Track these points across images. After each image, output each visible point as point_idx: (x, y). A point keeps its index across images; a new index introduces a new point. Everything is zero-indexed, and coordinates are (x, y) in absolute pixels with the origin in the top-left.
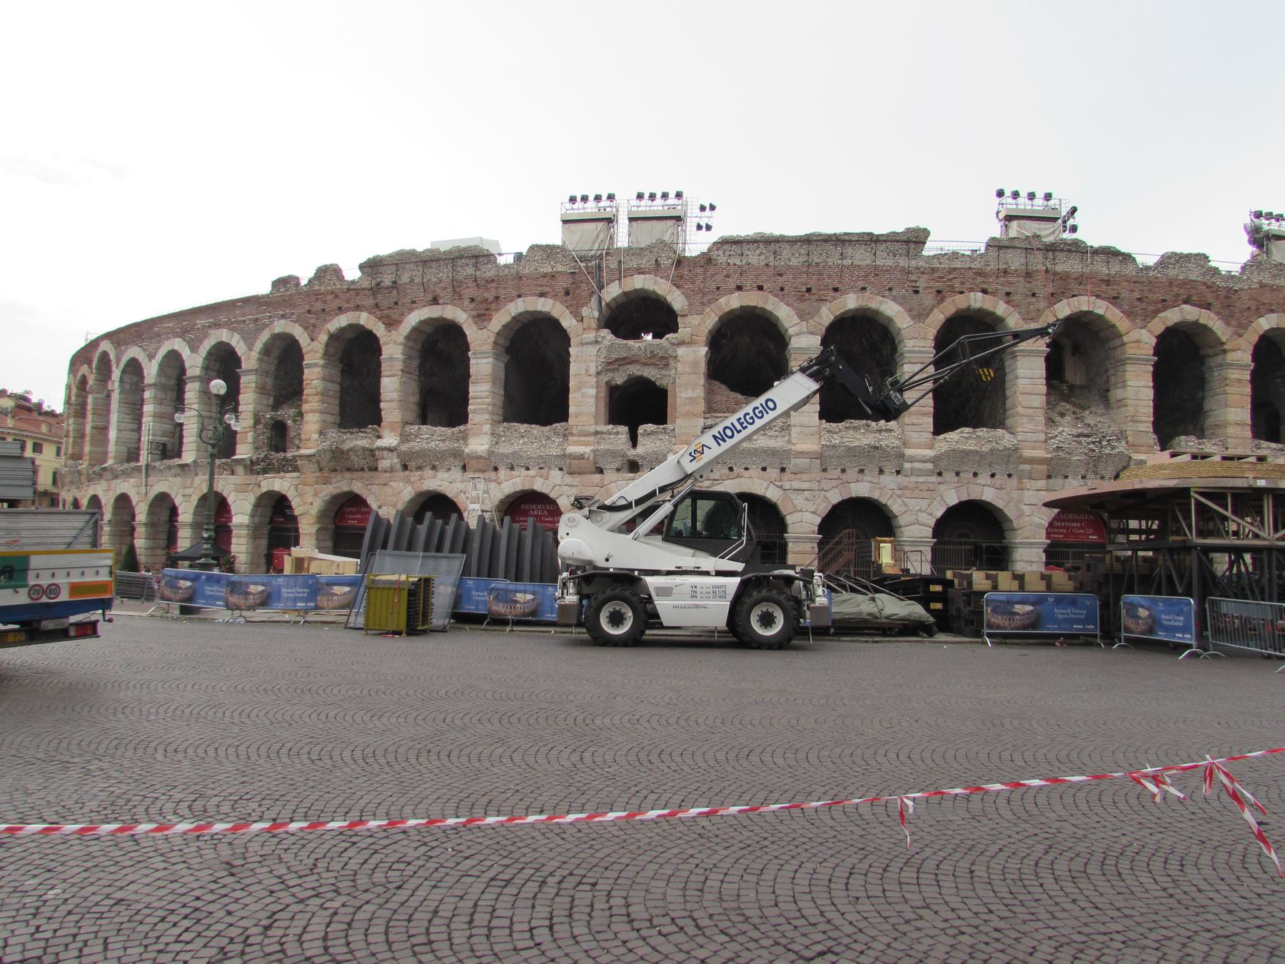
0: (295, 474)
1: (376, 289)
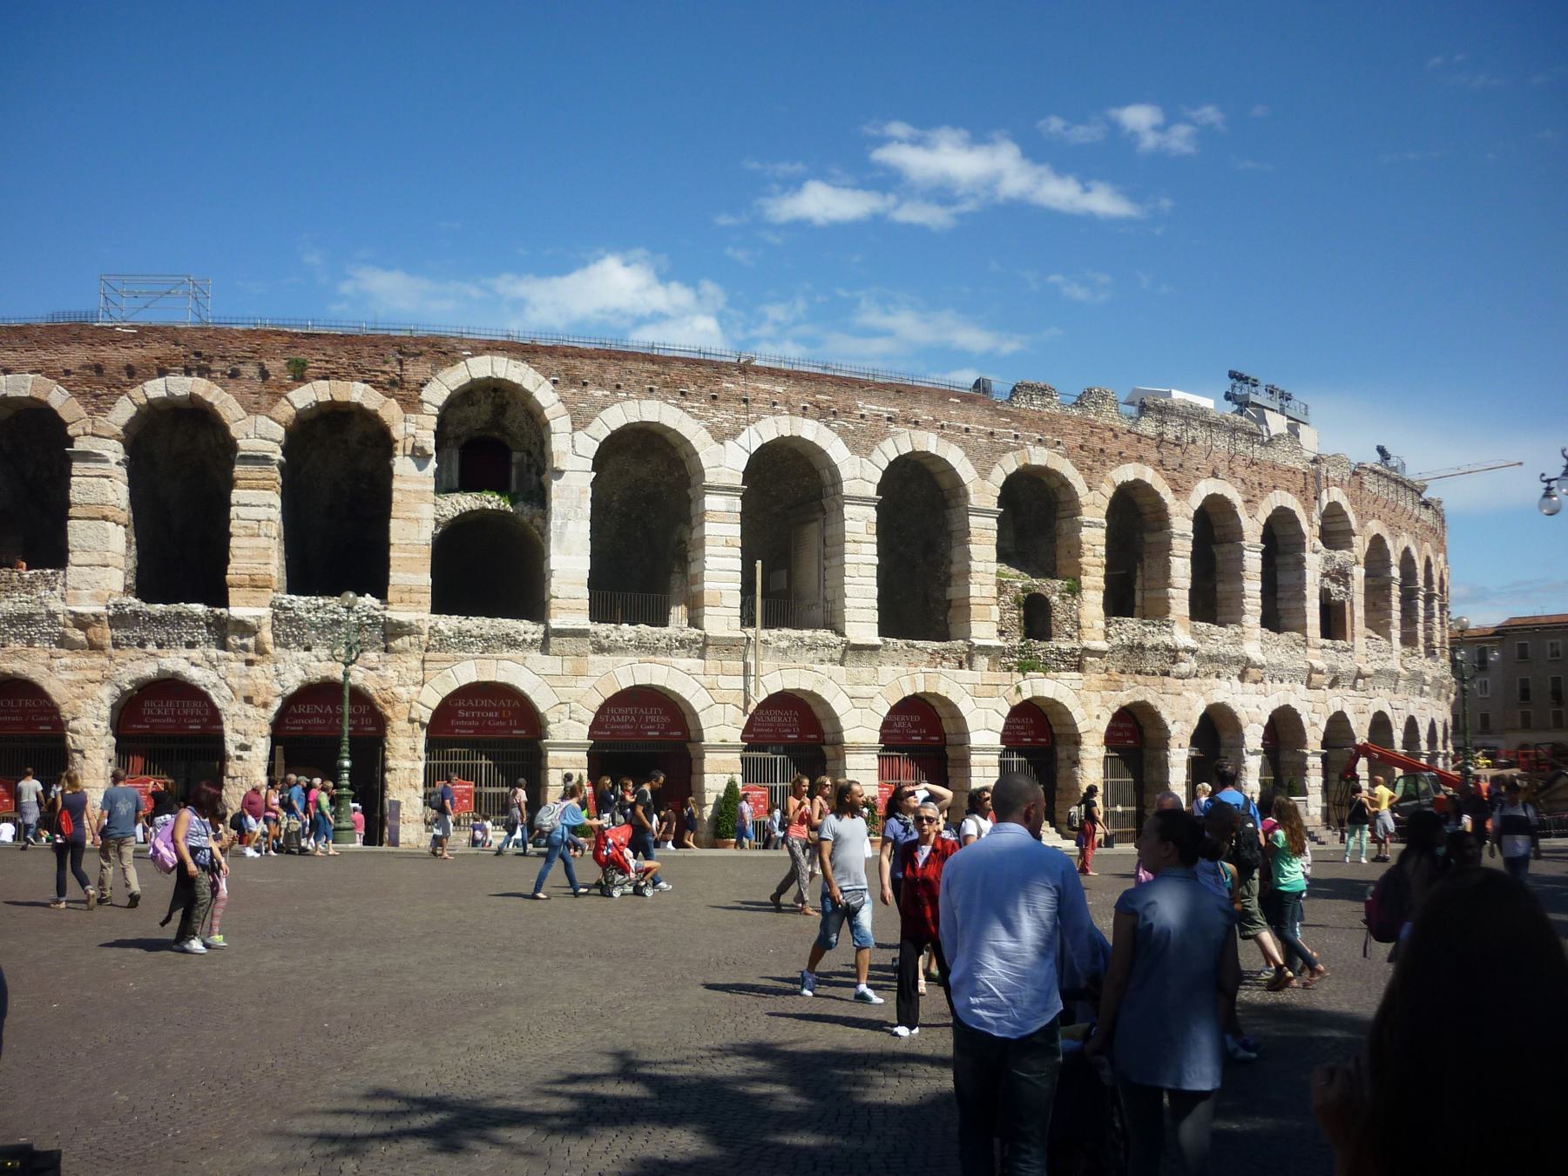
0: (1076, 675)
1: (1160, 440)
